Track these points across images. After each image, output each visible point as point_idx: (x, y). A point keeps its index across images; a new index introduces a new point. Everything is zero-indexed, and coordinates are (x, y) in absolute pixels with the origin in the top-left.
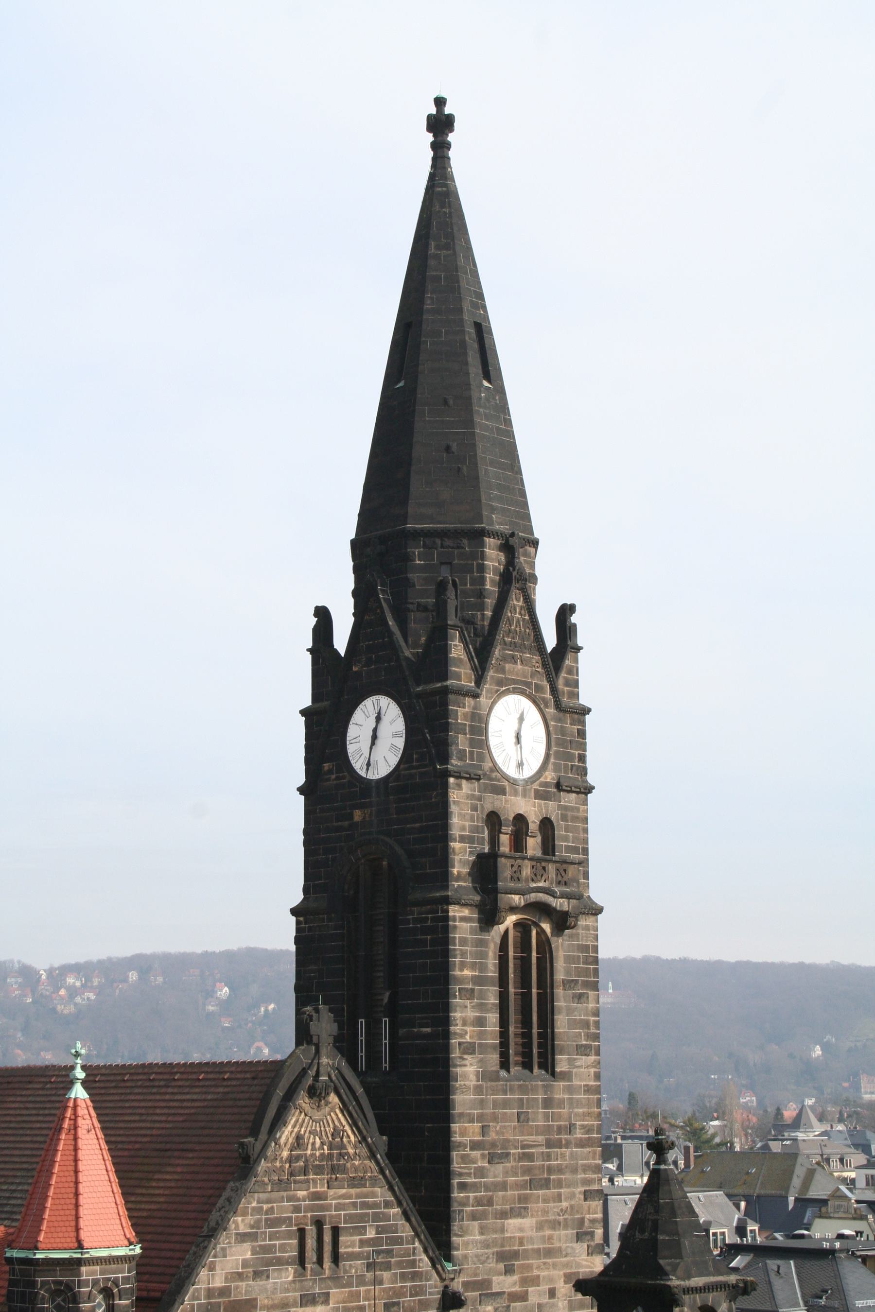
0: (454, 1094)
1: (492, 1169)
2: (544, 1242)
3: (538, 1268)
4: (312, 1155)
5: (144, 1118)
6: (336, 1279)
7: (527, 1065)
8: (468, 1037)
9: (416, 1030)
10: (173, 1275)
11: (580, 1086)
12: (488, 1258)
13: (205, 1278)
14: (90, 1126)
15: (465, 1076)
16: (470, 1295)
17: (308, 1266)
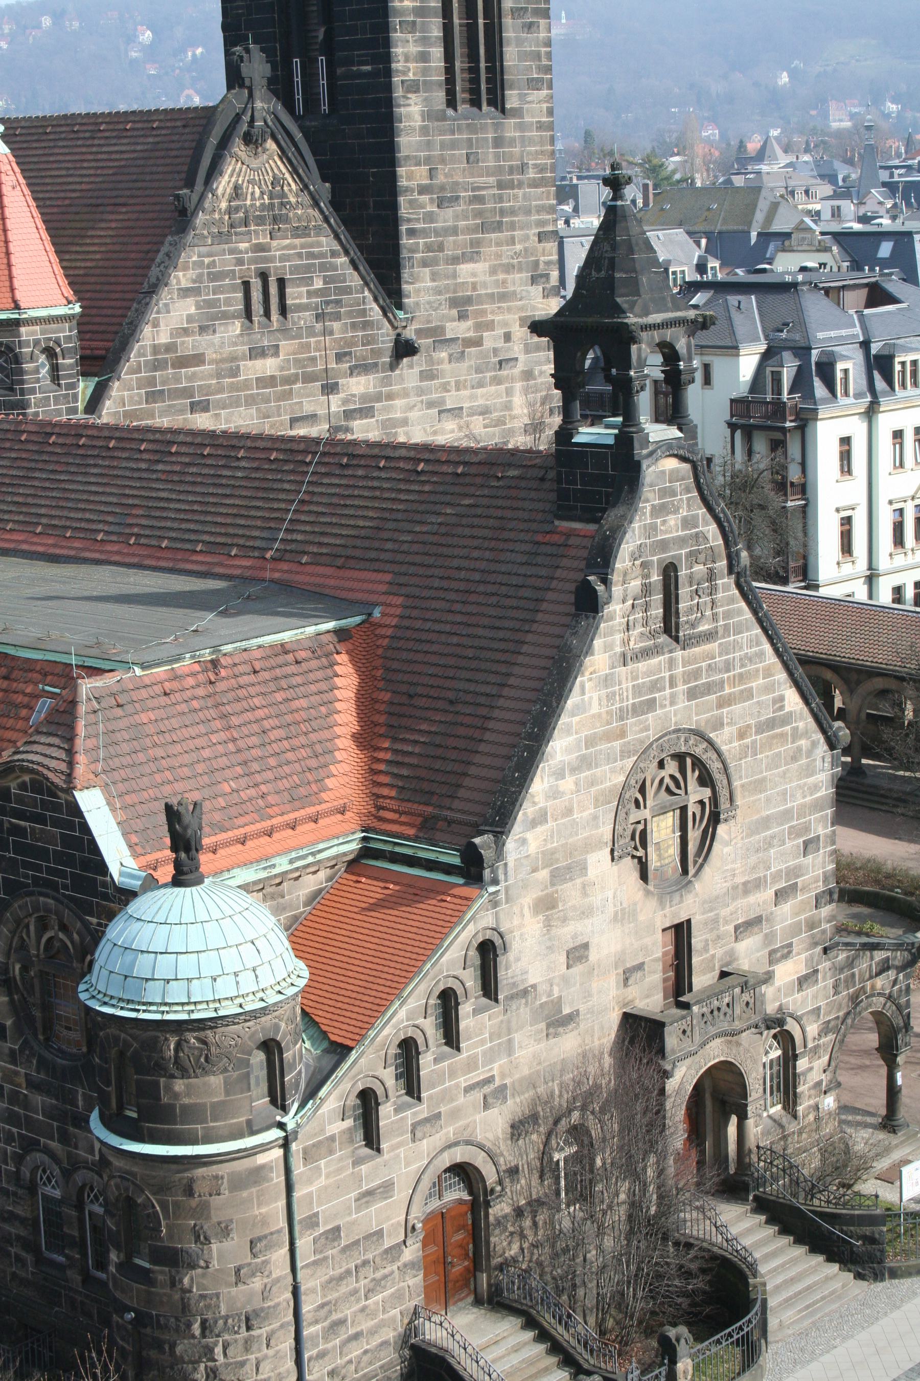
0: (399, 136)
1: (442, 214)
2: (498, 287)
3: (492, 312)
4: (252, 205)
5: (71, 172)
6: (284, 331)
7: (476, 102)
8: (411, 74)
9: (355, 69)
10: (116, 333)
11: (532, 123)
12: (440, 304)
13: (150, 335)
14: (15, 182)
15: (409, 117)
16: (423, 343)
17: (255, 319)
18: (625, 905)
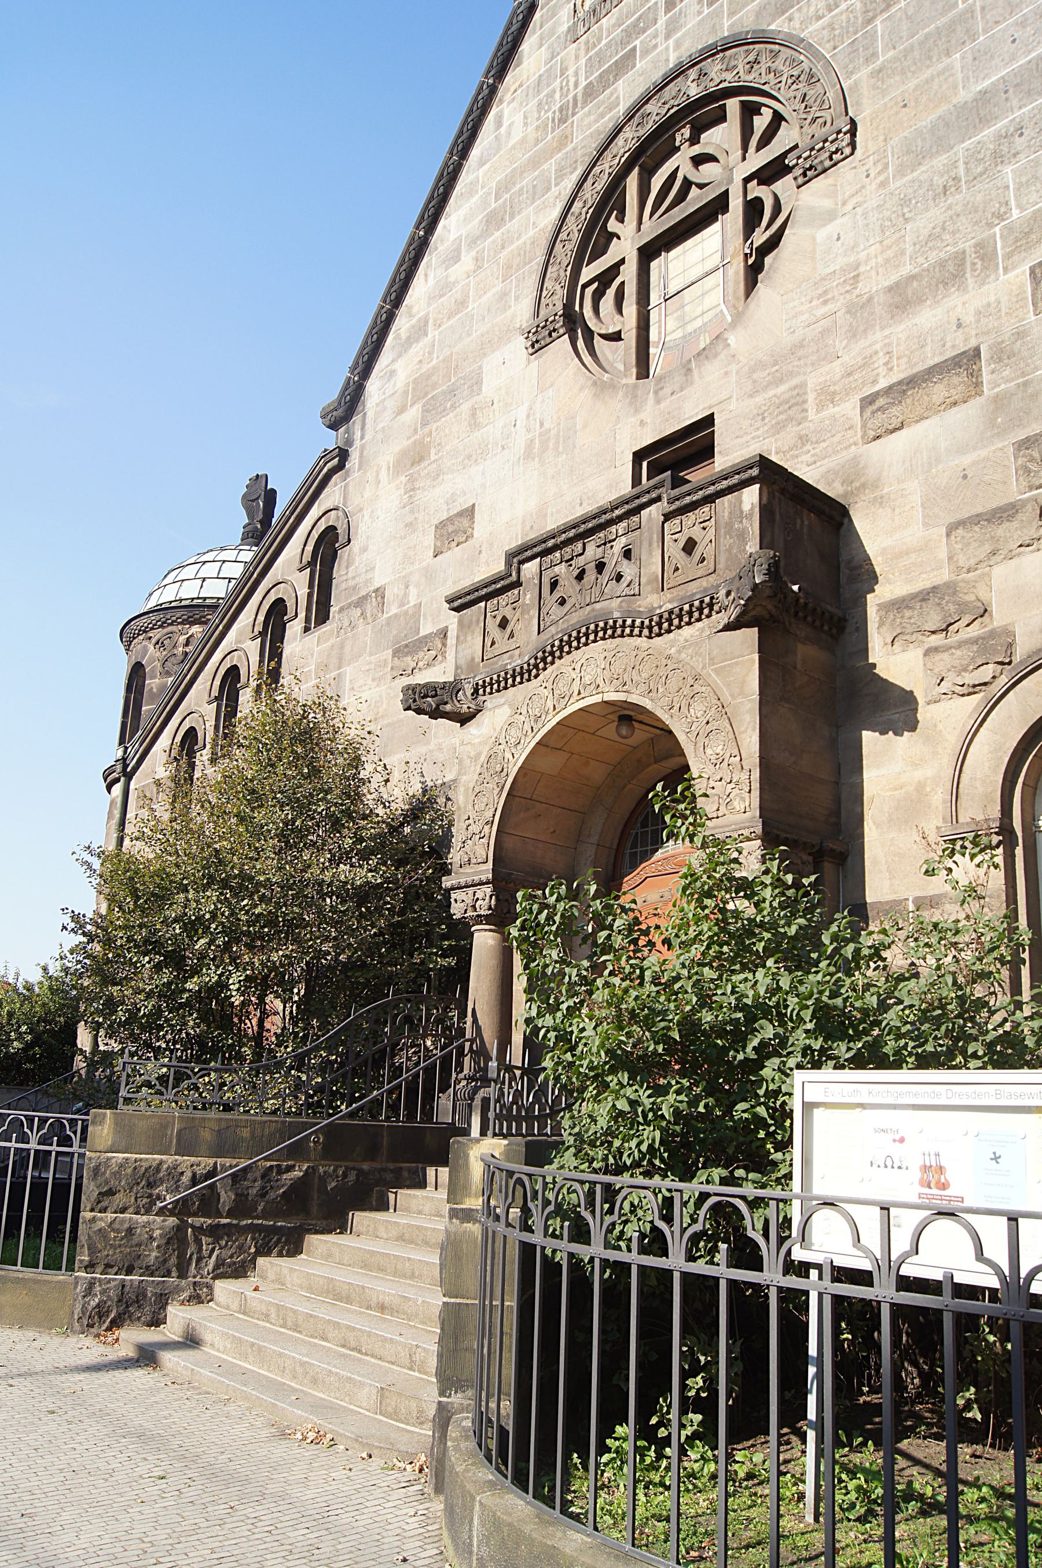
18: (547, 425)
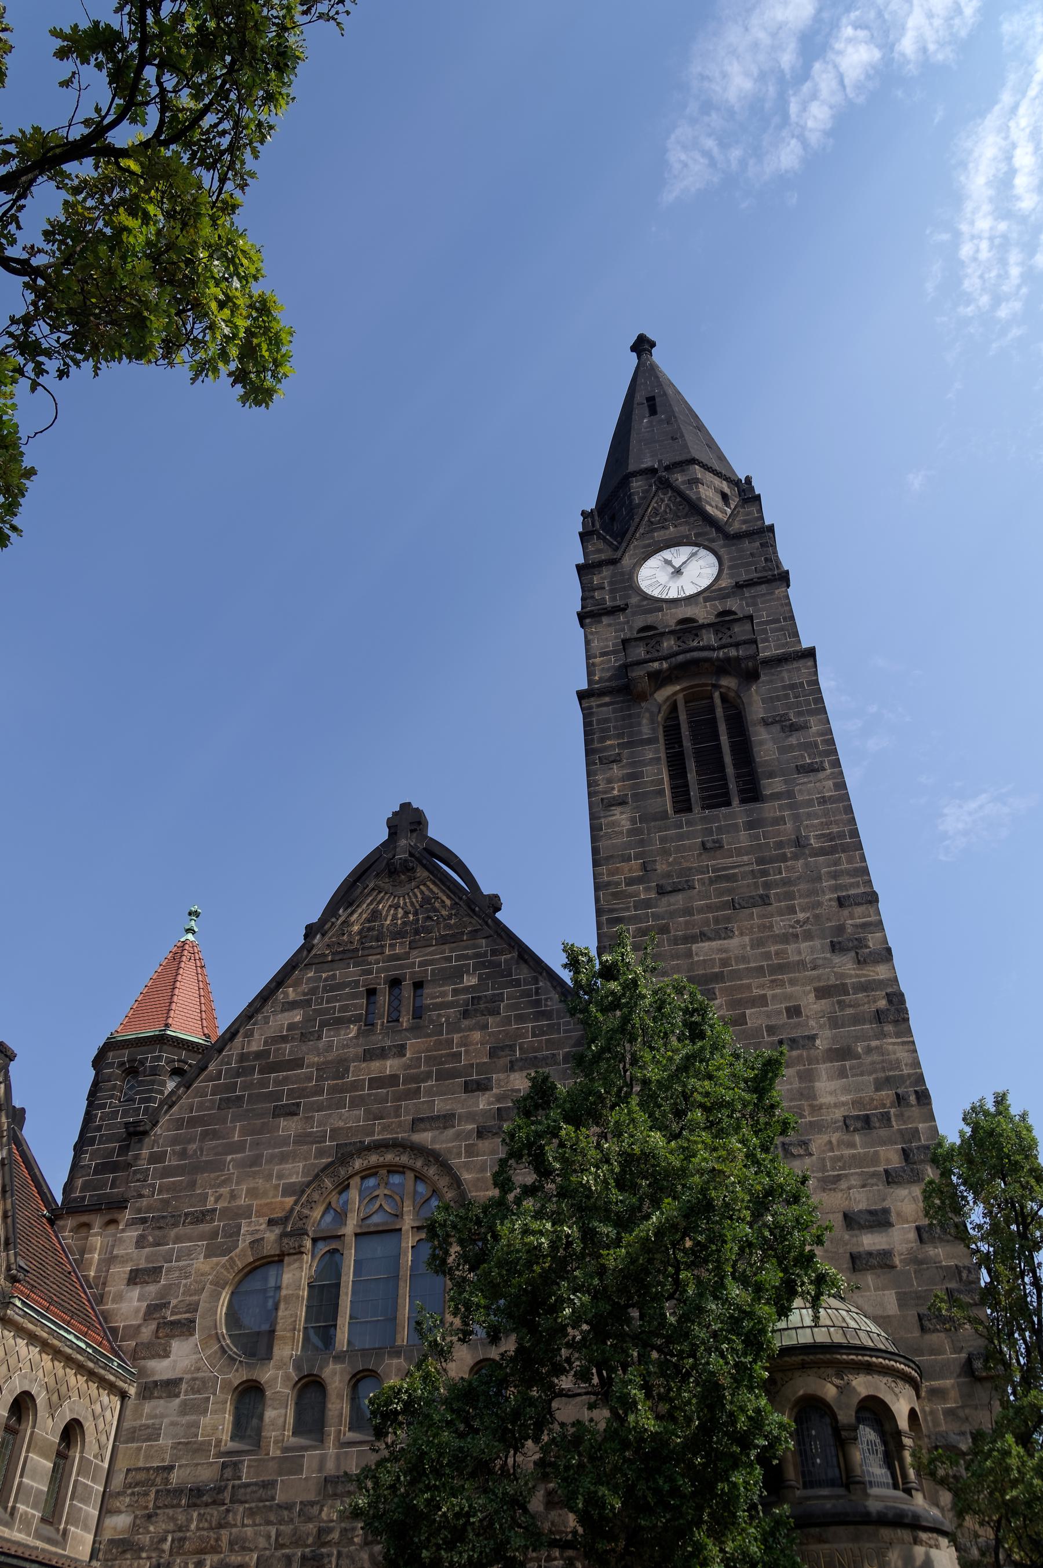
6: (415, 1030)
13: (239, 1045)
